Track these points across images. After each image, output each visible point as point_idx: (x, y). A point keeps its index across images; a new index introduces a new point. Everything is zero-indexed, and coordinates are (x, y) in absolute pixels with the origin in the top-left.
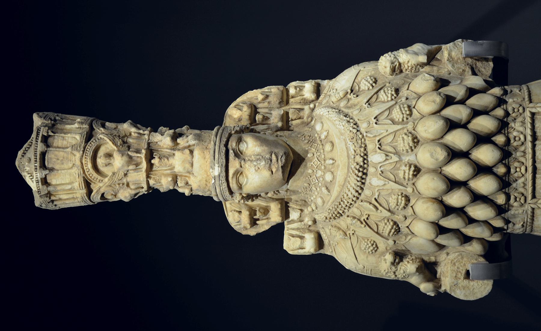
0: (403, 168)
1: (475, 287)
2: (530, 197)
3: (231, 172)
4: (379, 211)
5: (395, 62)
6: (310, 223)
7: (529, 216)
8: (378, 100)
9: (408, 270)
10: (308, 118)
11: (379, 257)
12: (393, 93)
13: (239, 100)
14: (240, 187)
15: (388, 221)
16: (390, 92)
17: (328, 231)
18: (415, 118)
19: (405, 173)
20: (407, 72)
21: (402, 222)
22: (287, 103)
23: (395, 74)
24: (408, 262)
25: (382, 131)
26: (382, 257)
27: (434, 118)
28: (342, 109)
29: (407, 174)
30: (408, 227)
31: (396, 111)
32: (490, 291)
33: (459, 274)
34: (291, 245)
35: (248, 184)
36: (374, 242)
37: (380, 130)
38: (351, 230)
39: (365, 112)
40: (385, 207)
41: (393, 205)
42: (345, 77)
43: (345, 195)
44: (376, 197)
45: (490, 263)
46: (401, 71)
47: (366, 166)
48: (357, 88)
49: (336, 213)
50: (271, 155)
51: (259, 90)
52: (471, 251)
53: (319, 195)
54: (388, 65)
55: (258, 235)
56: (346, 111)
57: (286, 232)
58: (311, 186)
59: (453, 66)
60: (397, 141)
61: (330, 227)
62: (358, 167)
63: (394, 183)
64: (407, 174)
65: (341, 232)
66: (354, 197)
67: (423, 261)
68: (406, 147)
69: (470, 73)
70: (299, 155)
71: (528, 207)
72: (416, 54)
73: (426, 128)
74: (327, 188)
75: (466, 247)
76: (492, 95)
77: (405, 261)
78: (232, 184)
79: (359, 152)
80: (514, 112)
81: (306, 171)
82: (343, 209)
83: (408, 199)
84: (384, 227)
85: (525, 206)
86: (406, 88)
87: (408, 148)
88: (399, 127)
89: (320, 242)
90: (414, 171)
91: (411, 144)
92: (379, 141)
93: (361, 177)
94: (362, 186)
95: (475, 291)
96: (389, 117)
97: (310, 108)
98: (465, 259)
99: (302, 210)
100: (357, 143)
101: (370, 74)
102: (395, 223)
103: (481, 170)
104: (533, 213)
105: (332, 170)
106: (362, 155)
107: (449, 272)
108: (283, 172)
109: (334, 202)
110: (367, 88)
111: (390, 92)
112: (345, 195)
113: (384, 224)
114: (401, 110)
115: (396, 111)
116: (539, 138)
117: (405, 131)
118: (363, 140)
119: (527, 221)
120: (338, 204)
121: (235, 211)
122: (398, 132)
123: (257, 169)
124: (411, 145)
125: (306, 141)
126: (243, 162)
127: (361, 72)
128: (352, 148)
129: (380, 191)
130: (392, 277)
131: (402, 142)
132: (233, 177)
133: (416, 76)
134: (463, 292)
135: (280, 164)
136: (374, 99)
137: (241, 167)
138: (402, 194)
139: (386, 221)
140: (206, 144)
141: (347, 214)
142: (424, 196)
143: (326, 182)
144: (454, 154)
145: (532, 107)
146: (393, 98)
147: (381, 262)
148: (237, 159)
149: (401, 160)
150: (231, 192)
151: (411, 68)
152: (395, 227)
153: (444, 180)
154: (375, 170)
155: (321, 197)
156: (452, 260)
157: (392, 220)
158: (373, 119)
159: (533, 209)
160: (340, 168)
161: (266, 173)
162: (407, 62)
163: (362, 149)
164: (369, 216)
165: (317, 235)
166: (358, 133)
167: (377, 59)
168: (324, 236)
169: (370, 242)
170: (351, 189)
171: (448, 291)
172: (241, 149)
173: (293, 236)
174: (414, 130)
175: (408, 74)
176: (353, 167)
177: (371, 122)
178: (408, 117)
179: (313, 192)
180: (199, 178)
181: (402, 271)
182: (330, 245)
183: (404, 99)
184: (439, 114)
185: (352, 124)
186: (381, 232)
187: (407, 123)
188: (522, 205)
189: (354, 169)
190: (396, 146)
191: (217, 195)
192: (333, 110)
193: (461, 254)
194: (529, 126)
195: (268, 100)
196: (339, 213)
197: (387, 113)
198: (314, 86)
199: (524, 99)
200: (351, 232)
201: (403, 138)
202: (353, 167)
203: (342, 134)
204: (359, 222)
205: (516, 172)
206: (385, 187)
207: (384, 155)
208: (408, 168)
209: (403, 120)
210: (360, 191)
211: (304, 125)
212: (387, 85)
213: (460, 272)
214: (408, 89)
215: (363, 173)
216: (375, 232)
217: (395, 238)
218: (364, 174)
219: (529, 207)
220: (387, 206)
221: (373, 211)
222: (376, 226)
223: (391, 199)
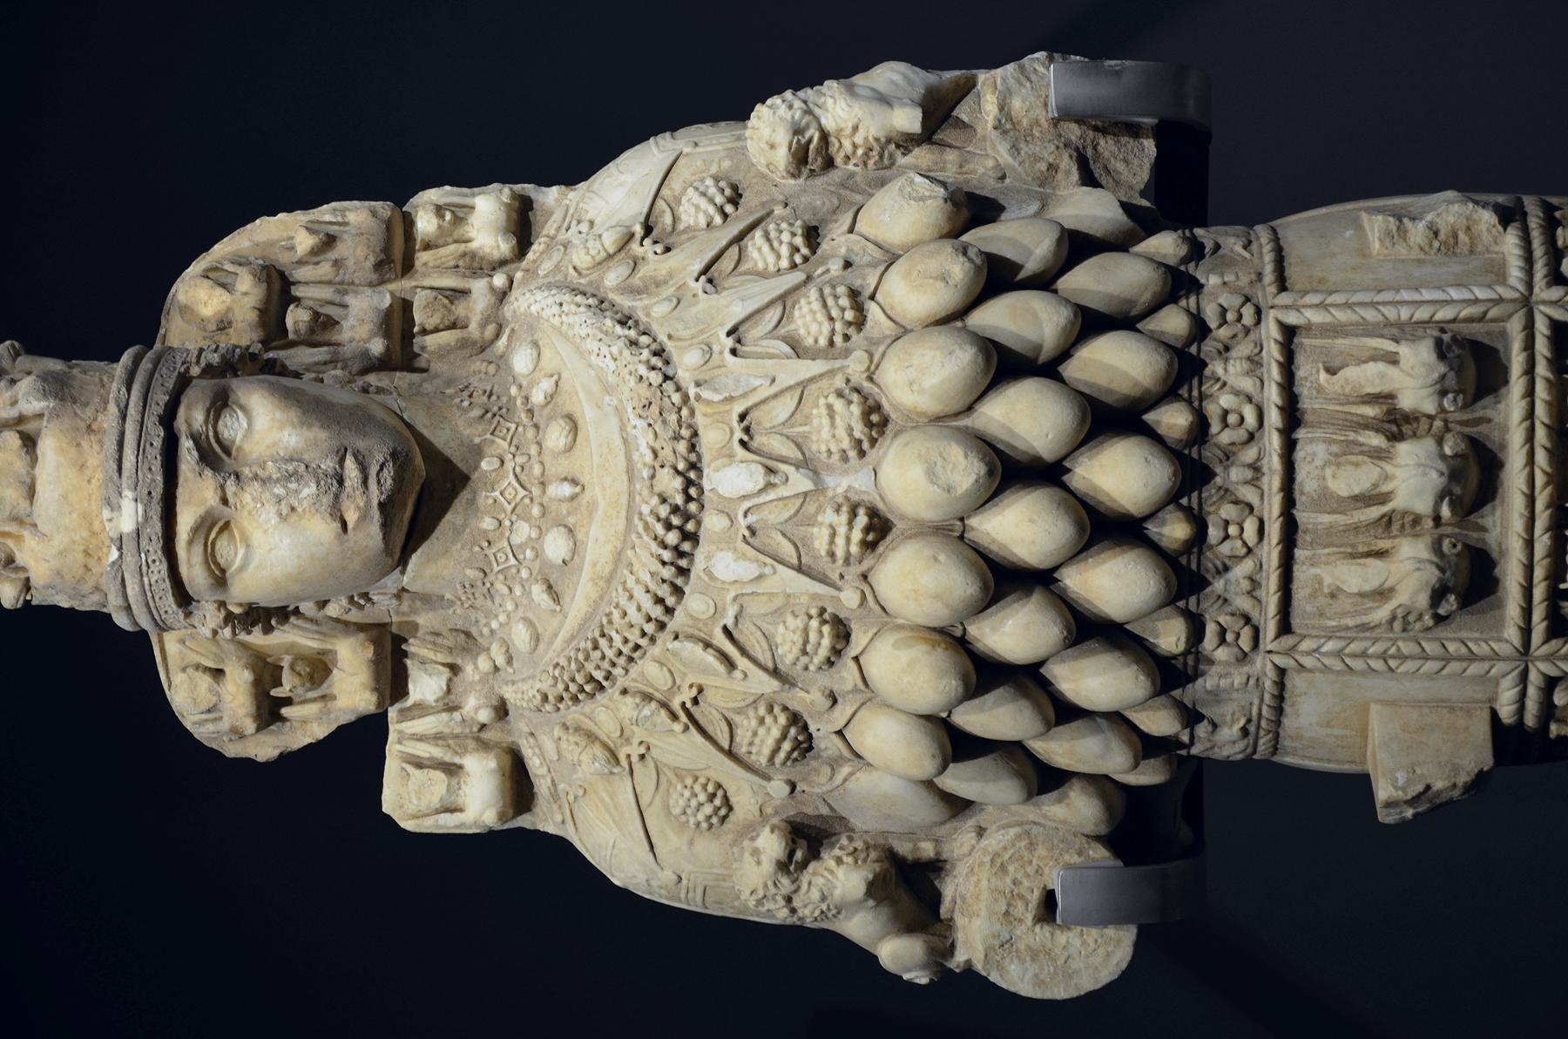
0: (829, 516)
1: (1072, 950)
2: (1270, 628)
3: (186, 520)
4: (738, 674)
5: (808, 126)
6: (485, 716)
7: (1267, 697)
8: (742, 268)
9: (838, 888)
10: (483, 325)
11: (735, 843)
12: (799, 241)
13: (222, 249)
14: (220, 579)
15: (770, 710)
16: (786, 237)
17: (549, 745)
18: (875, 334)
19: (833, 535)
20: (851, 167)
21: (821, 714)
22: (408, 267)
23: (805, 172)
24: (839, 861)
25: (757, 382)
26: (746, 843)
27: (943, 339)
28: (611, 296)
29: (840, 541)
30: (840, 733)
31: (805, 309)
32: (1124, 965)
33: (1020, 904)
34: (410, 797)
35: (251, 568)
36: (719, 786)
37: (748, 377)
38: (635, 741)
39: (694, 310)
40: (761, 658)
41: (788, 652)
42: (623, 178)
43: (616, 615)
44: (730, 622)
45: (1126, 864)
46: (829, 164)
47: (693, 507)
48: (668, 219)
49: (580, 679)
50: (342, 461)
51: (300, 217)
52: (1064, 822)
53: (520, 613)
54: (783, 138)
55: (286, 758)
56: (625, 302)
57: (393, 749)
58: (491, 577)
59: (1015, 149)
60: (807, 420)
61: (557, 731)
62: (664, 511)
63: (793, 573)
64: (840, 541)
65: (598, 750)
66: (649, 619)
67: (891, 856)
68: (839, 441)
69: (1075, 176)
70: (447, 461)
71: (1263, 666)
72: (884, 100)
73: (912, 373)
74: (550, 587)
75: (1045, 808)
76: (1150, 259)
77: (828, 858)
78: (190, 566)
79: (671, 458)
80: (1224, 322)
81: (473, 523)
82: (606, 665)
83: (843, 633)
84: (755, 734)
85: (1252, 663)
86: (846, 227)
87: (846, 443)
88: (818, 367)
89: (519, 785)
90: (867, 529)
91: (859, 431)
92: (742, 417)
93: (676, 548)
94: (679, 582)
95: (1075, 965)
96: (782, 331)
97: (492, 289)
98: (1041, 851)
99: (454, 669)
100: (664, 422)
101: (714, 170)
102: (795, 719)
103: (1103, 528)
104: (1281, 685)
105: (571, 520)
106: (681, 466)
107: (985, 895)
108: (386, 526)
109: (573, 637)
110: (703, 222)
111: (788, 237)
112: (616, 615)
113: (754, 722)
114: (825, 305)
115: (805, 309)
116: (1308, 417)
117: (839, 382)
118: (685, 412)
119: (1260, 715)
120: (589, 645)
121: (197, 667)
122: (813, 387)
124: (857, 434)
125: (477, 412)
126: (231, 486)
127: (681, 161)
128: (644, 439)
129: (744, 601)
130: (781, 915)
131: (826, 421)
132: (191, 542)
133: (882, 183)
134: (1033, 968)
135: (375, 495)
136: (727, 263)
137: (225, 501)
138: (823, 611)
139: (762, 711)
140: (89, 412)
141: (621, 682)
142: (900, 621)
143: (546, 564)
144: (1011, 471)
145: (1287, 307)
146: (798, 259)
147: (740, 859)
148: (208, 472)
149: (820, 489)
150: (184, 599)
151: (866, 154)
152: (793, 731)
153: (971, 565)
154: (725, 522)
155: (526, 620)
156: (997, 855)
157: (785, 709)
158: (722, 335)
159: (1282, 672)
160: (600, 514)
161: (321, 529)
162: (848, 131)
163: (682, 447)
164: (700, 691)
165: (507, 761)
166: (669, 386)
167: (743, 115)
168: (534, 764)
169: (705, 787)
170: (639, 593)
171: (979, 967)
172: (226, 434)
173: (419, 764)
174: (870, 379)
175: (852, 175)
176: (646, 510)
177: (716, 348)
178: (851, 331)
179: (497, 601)
180: (59, 541)
181: (815, 895)
182: (555, 796)
183: (835, 267)
184: (959, 324)
185: (646, 353)
186: (742, 750)
187: (846, 353)
188: (1243, 658)
189: (651, 520)
190: (806, 437)
191: (128, 608)
192: (579, 299)
193: (1028, 833)
194: (1275, 373)
195: (332, 255)
196: (591, 679)
197: (774, 315)
198: (508, 206)
199: (1260, 276)
200: (636, 751)
201: (830, 407)
202: (646, 510)
203: (608, 389)
204: (663, 712)
205: (1227, 537)
206: (760, 588)
207: (761, 470)
208: (844, 517)
209: (831, 343)
210: (670, 601)
211: (468, 352)
212: (778, 210)
213: (1021, 897)
214: (851, 231)
215: (683, 532)
216: (721, 749)
217: (795, 772)
218: (686, 536)
219: (1269, 666)
220: (768, 655)
221: (715, 674)
222: (725, 728)
223: (781, 629)
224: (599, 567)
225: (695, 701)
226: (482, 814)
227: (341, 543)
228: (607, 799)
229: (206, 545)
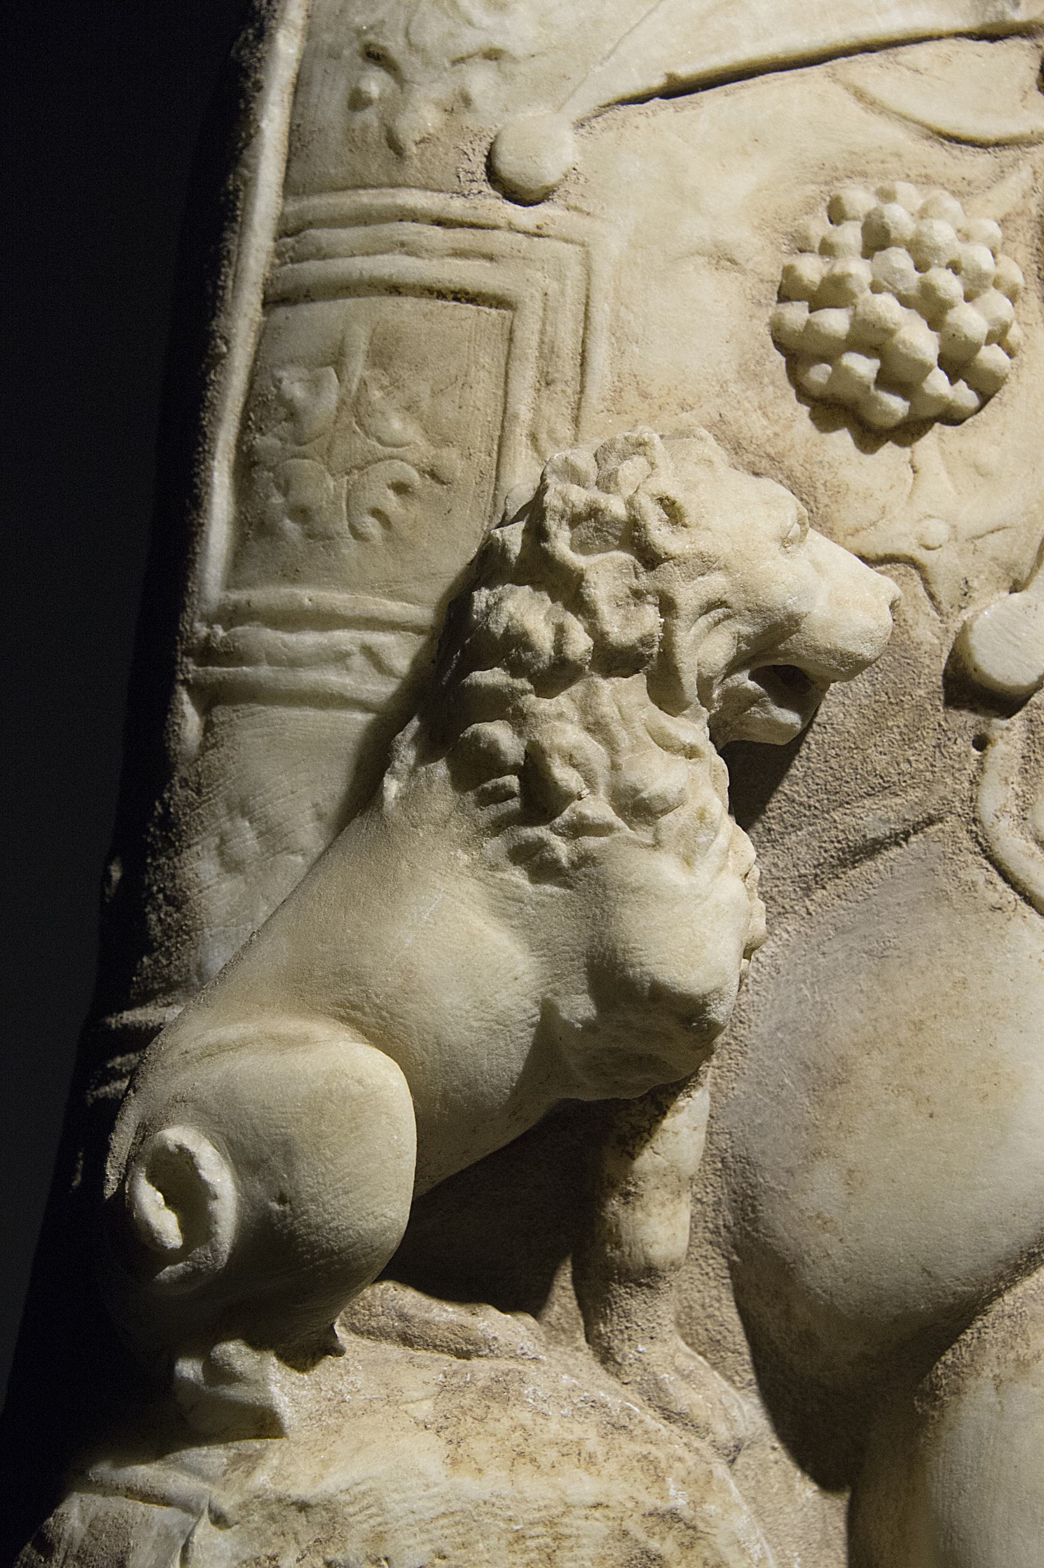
36: (988, 388)
107: (536, 1489)
181: (659, 775)
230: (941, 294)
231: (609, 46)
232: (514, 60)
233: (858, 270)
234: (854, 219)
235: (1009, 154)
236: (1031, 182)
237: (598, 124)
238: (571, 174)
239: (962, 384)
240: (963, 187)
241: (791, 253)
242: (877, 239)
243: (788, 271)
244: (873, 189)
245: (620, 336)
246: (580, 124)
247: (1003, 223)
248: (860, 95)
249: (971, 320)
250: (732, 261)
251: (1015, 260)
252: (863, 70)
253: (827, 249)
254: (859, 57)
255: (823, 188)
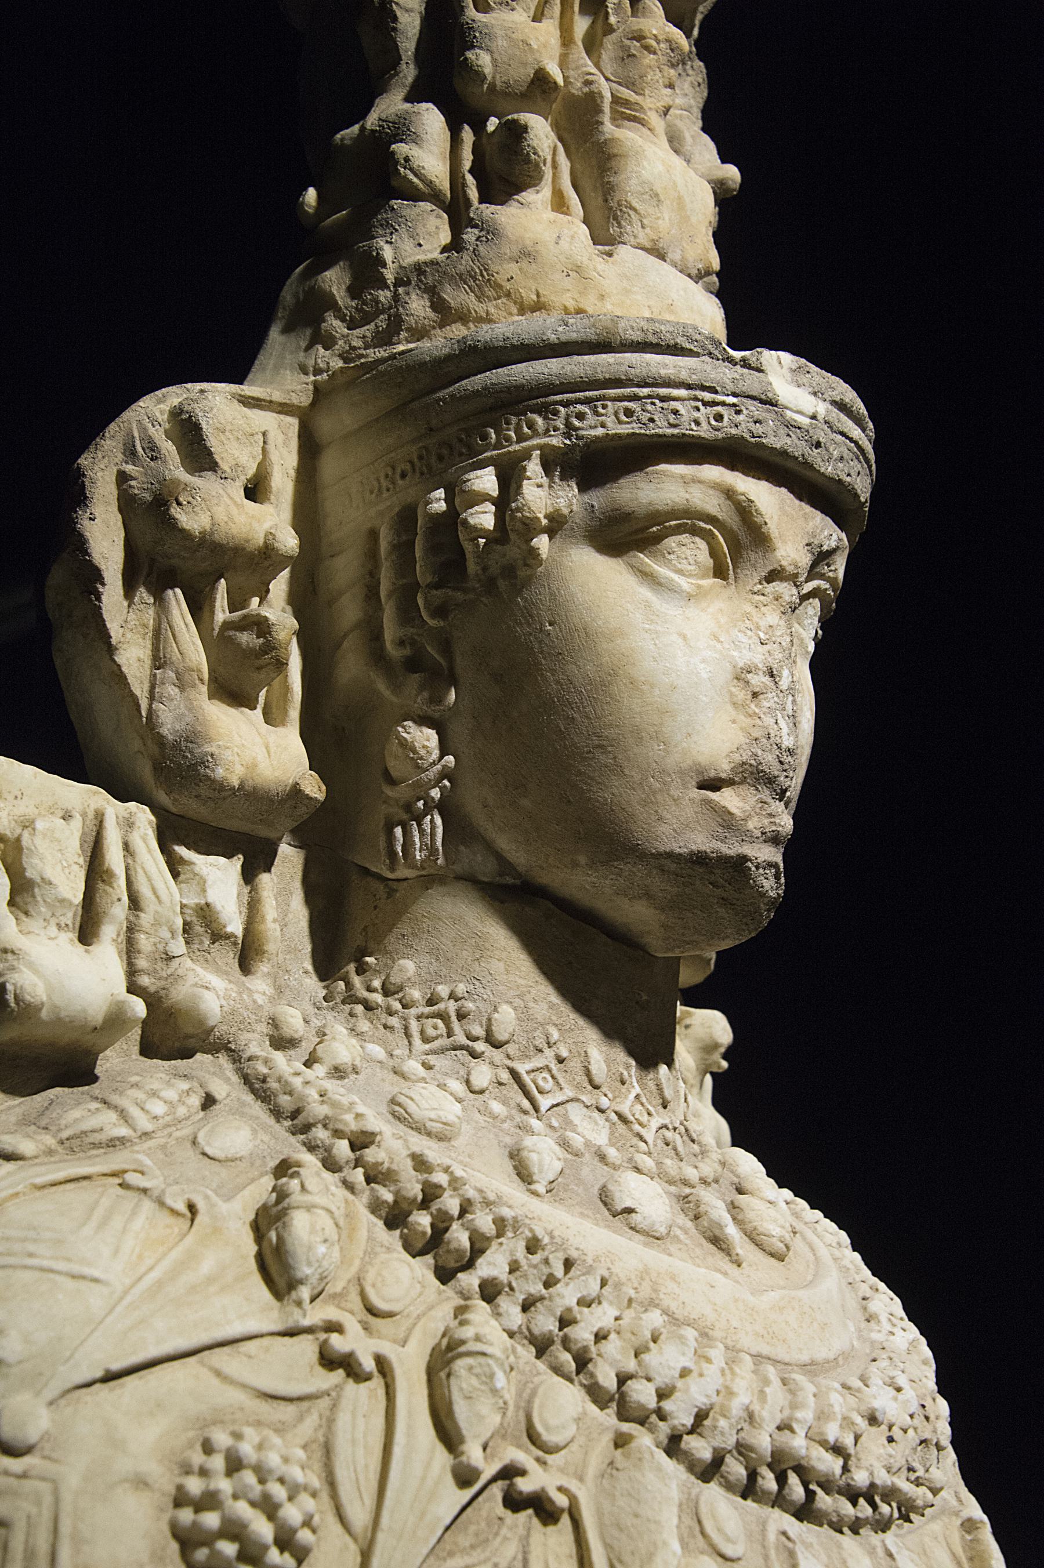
3: (766, 498)
14: (625, 536)
35: (645, 592)
66: (662, 1395)
108: (699, 859)
123: (759, 680)
126: (787, 591)
132: (729, 494)
137: (772, 577)
200: (353, 1341)
224: (671, 1286)
225: (514, 1502)
226: (31, 966)
227: (681, 773)
228: (207, 1266)
229: (712, 520)
230: (276, 1500)
231: (68, 1354)
232: (9, 1365)
233: (224, 1485)
234: (220, 1451)
235: (305, 1405)
236: (318, 1421)
237: (63, 1402)
238: (46, 1436)
239: (287, 1555)
240: (279, 1426)
241: (180, 1475)
242: (234, 1465)
243: (180, 1488)
244: (228, 1431)
245: (77, 1540)
246: (51, 1403)
247: (304, 1447)
248: (218, 1373)
249: (292, 1513)
250: (146, 1484)
251: (313, 1471)
252: (219, 1358)
253: (204, 1472)
254: (217, 1350)
255: (200, 1432)
